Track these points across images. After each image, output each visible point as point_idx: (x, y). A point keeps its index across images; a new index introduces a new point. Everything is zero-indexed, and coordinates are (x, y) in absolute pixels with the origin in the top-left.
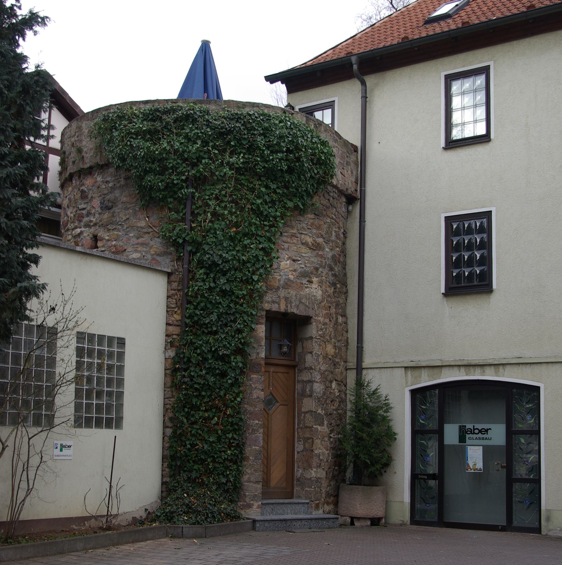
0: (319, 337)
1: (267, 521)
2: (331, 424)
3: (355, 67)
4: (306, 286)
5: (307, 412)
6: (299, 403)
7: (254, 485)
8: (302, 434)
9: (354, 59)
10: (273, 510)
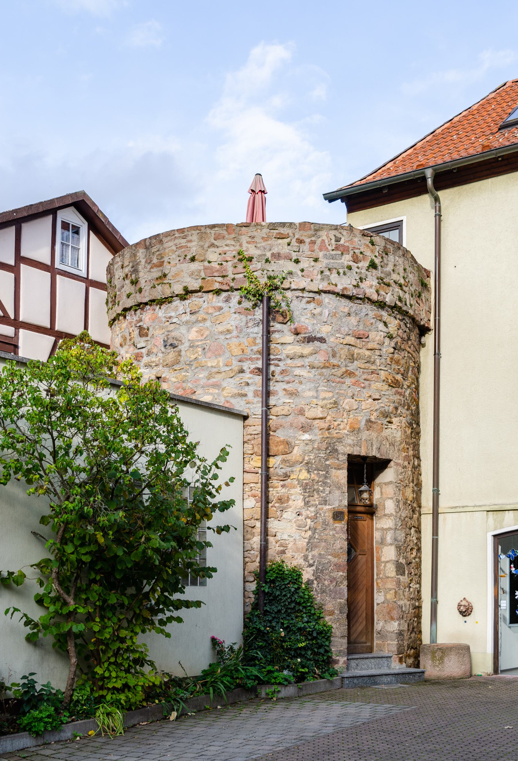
0: (399, 482)
1: (356, 677)
2: (411, 574)
3: (430, 182)
4: (386, 427)
5: (387, 562)
6: (378, 552)
7: (340, 640)
8: (382, 585)
9: (429, 173)
10: (357, 665)
